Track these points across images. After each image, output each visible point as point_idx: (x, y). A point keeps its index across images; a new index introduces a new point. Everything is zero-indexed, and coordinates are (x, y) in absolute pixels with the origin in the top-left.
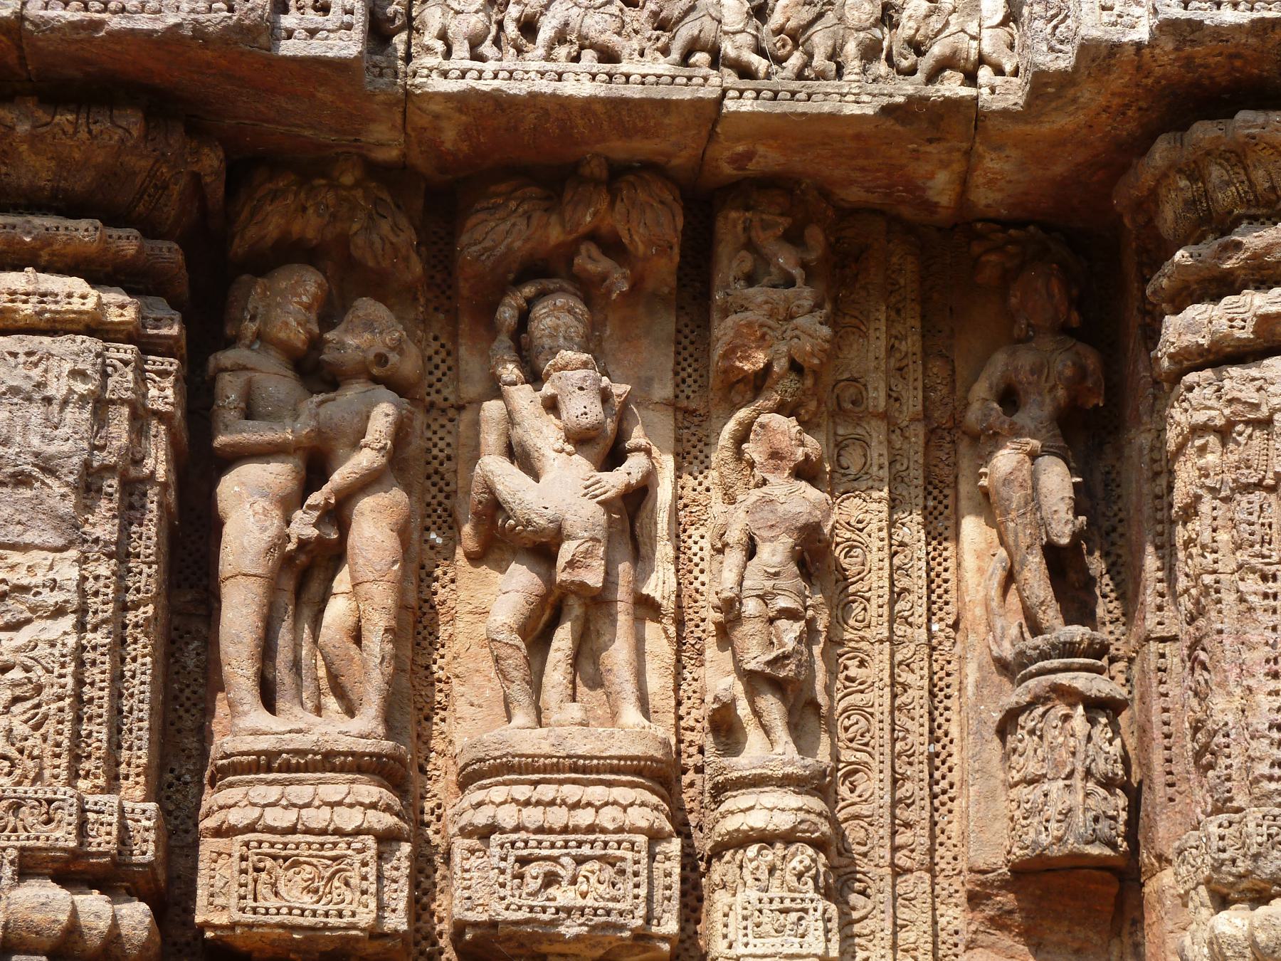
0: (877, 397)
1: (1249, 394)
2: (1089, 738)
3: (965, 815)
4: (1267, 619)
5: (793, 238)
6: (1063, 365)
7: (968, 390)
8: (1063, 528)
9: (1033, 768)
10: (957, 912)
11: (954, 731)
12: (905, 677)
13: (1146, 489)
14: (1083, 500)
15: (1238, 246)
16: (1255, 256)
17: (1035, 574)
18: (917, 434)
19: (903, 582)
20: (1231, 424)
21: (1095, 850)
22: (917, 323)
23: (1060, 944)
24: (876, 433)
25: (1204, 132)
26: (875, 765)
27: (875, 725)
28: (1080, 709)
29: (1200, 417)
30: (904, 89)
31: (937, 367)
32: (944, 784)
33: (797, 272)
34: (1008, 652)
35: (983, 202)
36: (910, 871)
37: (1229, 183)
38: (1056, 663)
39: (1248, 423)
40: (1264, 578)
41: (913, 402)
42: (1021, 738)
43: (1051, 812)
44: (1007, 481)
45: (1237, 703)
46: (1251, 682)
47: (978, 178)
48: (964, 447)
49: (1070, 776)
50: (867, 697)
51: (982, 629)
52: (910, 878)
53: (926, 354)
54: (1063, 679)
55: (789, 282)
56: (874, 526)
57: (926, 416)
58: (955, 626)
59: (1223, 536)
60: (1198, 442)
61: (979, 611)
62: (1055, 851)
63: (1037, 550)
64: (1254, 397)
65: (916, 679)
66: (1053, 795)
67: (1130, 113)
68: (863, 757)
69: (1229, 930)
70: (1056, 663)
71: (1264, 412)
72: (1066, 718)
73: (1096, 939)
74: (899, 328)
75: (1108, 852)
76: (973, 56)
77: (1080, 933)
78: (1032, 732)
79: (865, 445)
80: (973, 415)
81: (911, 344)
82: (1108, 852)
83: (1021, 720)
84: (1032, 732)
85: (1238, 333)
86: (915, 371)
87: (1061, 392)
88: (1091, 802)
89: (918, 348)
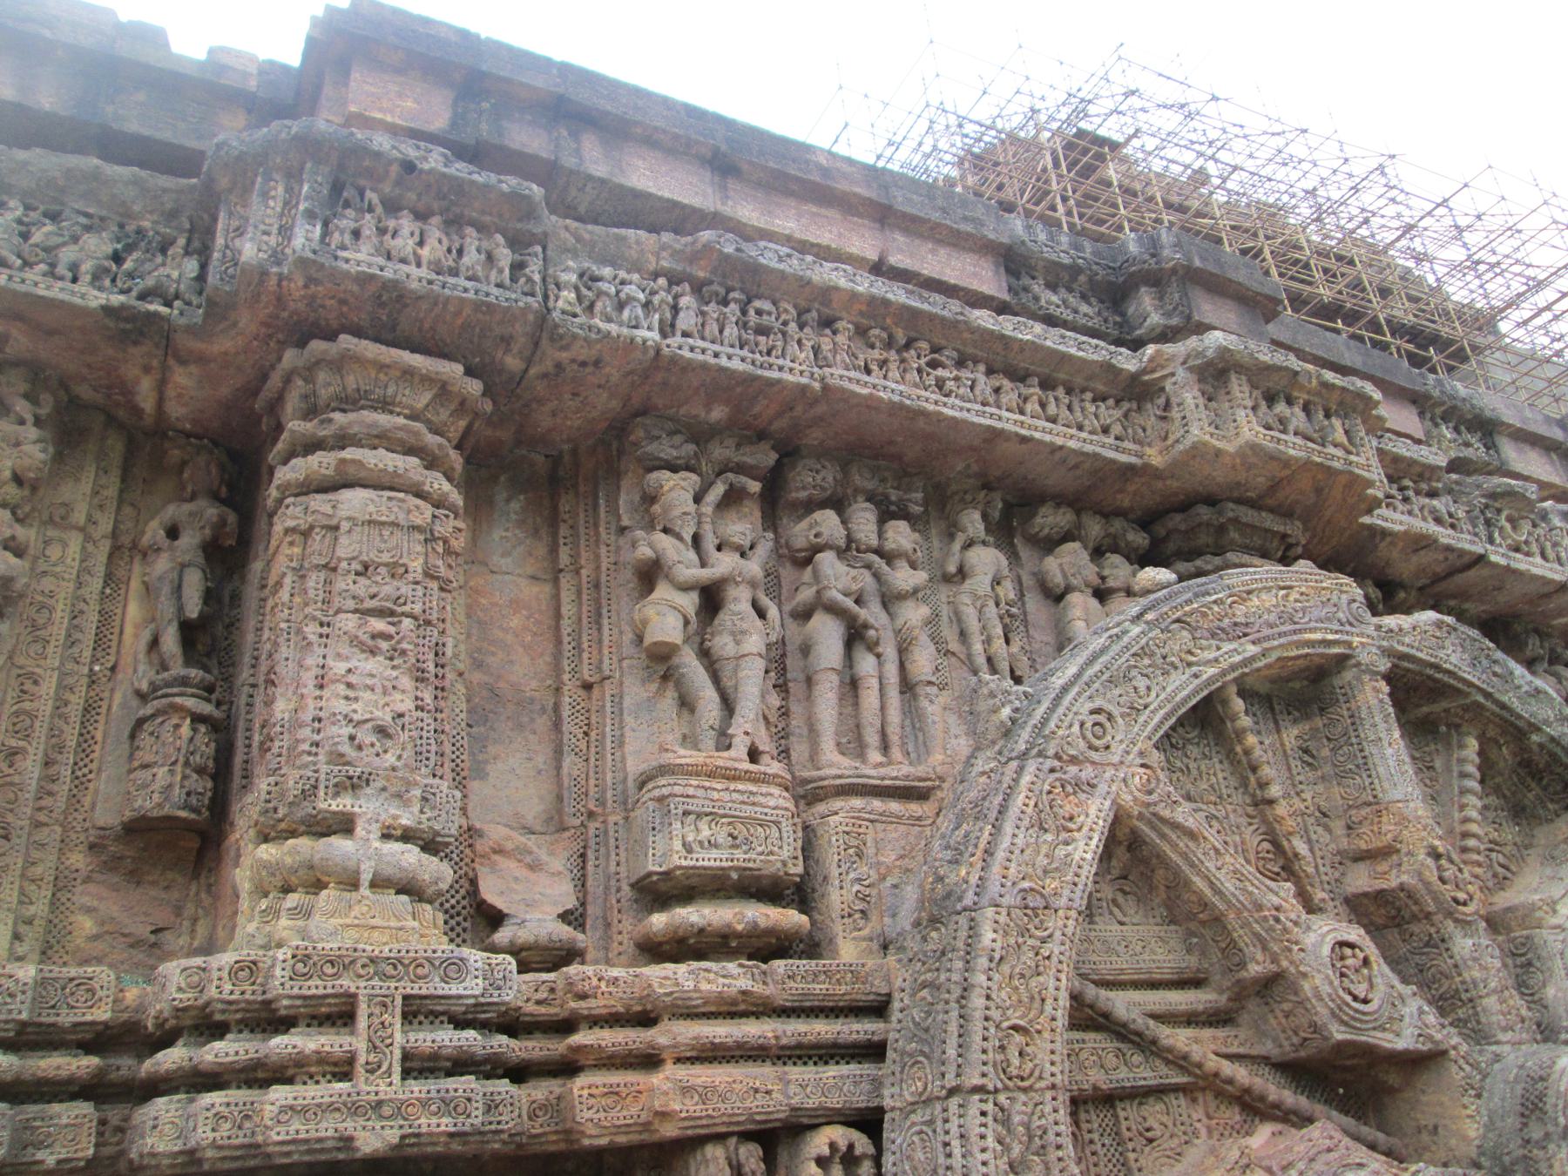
0: (79, 517)
1: (328, 509)
2: (191, 740)
3: (96, 791)
4: (321, 651)
5: (28, 396)
6: (212, 512)
7: (146, 524)
8: (193, 610)
9: (149, 758)
10: (80, 857)
11: (99, 736)
12: (68, 695)
13: (256, 594)
14: (209, 596)
15: (330, 421)
16: (341, 428)
17: (171, 642)
18: (105, 546)
19: (78, 635)
20: (312, 528)
21: (183, 814)
22: (118, 480)
23: (153, 883)
24: (75, 542)
25: (317, 346)
26: (31, 750)
27: (37, 724)
28: (188, 721)
29: (291, 523)
30: (117, 299)
31: (127, 510)
32: (85, 770)
33: (29, 418)
34: (144, 686)
35: (174, 415)
36: (46, 825)
37: (329, 384)
38: (175, 690)
39: (323, 527)
40: (322, 625)
41: (105, 524)
42: (144, 739)
43: (157, 786)
44: (160, 578)
45: (292, 706)
46: (304, 691)
47: (171, 392)
48: (138, 559)
49: (174, 763)
50: (35, 704)
51: (130, 671)
52: (46, 830)
53: (121, 501)
54: (178, 700)
55: (22, 422)
56: (63, 595)
57: (114, 535)
58: (113, 669)
59: (297, 600)
60: (289, 539)
61: (130, 660)
62: (155, 813)
63: (175, 624)
64: (330, 511)
65: (76, 701)
66: (160, 775)
67: (272, 344)
68: (21, 743)
69: (265, 856)
70: (175, 690)
71: (334, 522)
72: (177, 726)
73: (180, 879)
74: (103, 481)
75: (193, 816)
76: (172, 290)
77: (170, 875)
78: (152, 734)
79: (65, 545)
80: (145, 540)
81: (112, 492)
82: (193, 816)
83: (145, 726)
84: (152, 734)
85: (323, 471)
86: (112, 506)
87: (207, 531)
88: (186, 783)
89: (116, 494)
